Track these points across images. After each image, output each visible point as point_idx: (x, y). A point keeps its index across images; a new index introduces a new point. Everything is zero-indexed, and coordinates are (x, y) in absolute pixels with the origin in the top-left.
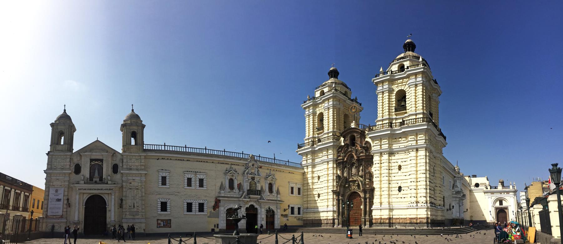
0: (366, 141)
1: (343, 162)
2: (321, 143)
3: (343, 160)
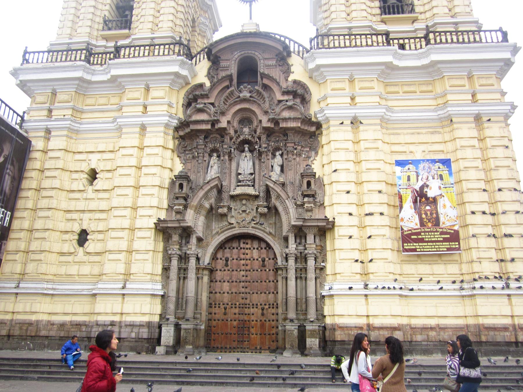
0: (295, 82)
1: (207, 134)
3: (213, 125)
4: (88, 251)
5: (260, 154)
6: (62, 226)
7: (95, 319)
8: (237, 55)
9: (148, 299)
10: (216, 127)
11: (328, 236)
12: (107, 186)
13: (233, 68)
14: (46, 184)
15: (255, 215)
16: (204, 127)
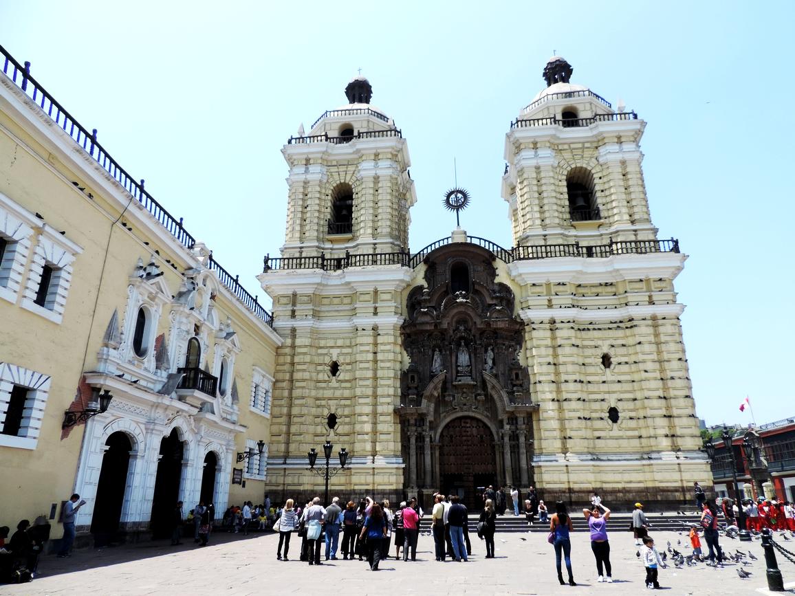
0: (501, 285)
1: (430, 334)
3: (436, 326)
4: (338, 431)
5: (476, 349)
6: (314, 411)
7: (352, 488)
8: (450, 261)
9: (394, 471)
10: (439, 328)
11: (534, 418)
12: (347, 376)
13: (447, 273)
15: (474, 401)
16: (428, 328)
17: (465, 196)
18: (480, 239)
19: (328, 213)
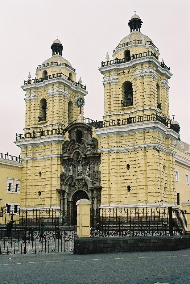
0: (93, 138)
1: (69, 159)
2: (44, 137)
3: (69, 157)
8: (76, 130)
14: (28, 178)
17: (83, 101)
18: (88, 119)
19: (38, 113)
